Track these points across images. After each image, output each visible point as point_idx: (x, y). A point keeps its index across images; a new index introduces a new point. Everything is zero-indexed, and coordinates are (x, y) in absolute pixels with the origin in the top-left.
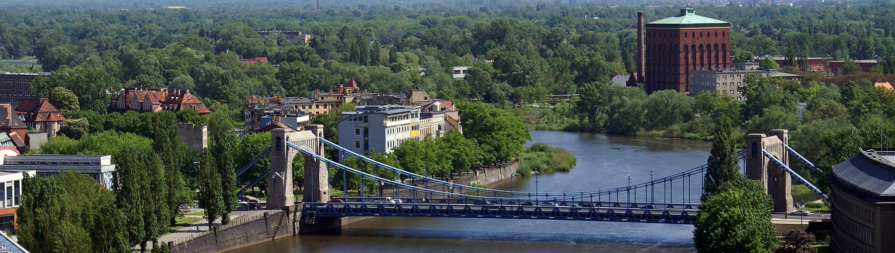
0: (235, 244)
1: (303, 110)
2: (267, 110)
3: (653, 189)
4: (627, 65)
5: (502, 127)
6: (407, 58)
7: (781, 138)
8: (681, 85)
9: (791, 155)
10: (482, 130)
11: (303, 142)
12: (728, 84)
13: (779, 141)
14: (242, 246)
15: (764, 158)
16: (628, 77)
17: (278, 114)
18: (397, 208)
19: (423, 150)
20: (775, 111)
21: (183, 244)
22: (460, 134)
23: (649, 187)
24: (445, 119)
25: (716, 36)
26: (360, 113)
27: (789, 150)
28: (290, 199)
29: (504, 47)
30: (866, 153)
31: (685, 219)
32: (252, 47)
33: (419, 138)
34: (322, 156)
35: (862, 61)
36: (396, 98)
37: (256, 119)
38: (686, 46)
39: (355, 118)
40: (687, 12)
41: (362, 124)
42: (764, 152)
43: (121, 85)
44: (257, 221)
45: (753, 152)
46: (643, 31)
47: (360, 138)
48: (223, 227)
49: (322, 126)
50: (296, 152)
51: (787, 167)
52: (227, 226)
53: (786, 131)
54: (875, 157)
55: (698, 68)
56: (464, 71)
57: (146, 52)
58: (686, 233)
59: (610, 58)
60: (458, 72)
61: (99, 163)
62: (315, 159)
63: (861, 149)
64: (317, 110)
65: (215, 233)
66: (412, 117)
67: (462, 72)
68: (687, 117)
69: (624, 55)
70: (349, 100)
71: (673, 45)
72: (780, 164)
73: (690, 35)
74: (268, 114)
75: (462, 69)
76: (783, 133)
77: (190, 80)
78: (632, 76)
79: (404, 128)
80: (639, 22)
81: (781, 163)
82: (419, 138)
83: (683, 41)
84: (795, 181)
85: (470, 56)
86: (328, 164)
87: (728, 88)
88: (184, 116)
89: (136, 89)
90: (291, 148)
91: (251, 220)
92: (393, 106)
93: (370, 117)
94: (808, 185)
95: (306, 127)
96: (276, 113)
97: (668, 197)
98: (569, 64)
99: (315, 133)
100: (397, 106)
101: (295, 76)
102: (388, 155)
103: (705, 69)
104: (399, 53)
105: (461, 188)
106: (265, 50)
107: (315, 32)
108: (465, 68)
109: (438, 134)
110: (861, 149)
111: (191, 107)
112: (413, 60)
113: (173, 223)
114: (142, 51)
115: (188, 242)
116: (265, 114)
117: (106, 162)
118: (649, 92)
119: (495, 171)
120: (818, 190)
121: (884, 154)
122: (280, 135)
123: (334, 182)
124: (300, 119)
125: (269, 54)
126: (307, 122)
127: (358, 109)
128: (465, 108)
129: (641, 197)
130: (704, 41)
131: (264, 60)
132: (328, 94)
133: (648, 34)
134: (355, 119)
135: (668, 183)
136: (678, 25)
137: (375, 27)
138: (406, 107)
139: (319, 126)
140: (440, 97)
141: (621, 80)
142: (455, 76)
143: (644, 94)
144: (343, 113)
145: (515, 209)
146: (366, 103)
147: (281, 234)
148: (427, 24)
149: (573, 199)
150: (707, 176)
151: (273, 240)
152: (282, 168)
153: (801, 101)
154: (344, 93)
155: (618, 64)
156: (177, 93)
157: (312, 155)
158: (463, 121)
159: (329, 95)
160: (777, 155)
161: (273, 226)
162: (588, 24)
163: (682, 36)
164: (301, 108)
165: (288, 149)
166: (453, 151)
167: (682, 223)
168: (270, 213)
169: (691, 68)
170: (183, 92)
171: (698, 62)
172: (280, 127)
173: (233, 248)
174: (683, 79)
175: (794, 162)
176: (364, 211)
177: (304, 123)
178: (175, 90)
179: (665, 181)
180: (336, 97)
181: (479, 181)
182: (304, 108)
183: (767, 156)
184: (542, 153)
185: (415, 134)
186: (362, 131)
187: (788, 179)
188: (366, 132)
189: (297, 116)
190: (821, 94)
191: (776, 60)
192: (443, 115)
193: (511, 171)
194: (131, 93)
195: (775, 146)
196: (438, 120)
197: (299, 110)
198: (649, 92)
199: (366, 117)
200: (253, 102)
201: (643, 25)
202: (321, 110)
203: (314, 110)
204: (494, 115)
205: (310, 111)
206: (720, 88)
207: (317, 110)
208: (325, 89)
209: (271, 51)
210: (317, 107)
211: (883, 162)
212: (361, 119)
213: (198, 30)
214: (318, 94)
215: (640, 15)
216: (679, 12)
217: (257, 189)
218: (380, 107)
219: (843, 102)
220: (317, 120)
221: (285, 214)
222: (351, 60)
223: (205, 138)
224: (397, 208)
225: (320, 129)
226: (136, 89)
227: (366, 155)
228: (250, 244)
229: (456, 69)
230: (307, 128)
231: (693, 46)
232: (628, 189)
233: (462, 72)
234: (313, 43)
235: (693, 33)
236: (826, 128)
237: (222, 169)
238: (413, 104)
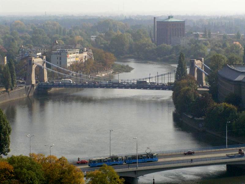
3: (158, 78)
7: (202, 61)
9: (205, 67)
11: (39, 62)
13: (201, 62)
23: (157, 78)
24: (88, 54)
27: (204, 65)
28: (34, 82)
30: (229, 66)
35: (230, 34)
39: (56, 54)
41: (59, 56)
47: (58, 60)
49: (45, 56)
50: (36, 65)
51: (203, 70)
53: (203, 58)
56: (95, 37)
58: (168, 94)
60: (93, 38)
64: (44, 51)
74: (27, 52)
75: (94, 36)
76: (202, 59)
93: (62, 54)
95: (41, 57)
97: (163, 81)
99: (43, 59)
100: (71, 49)
105: (93, 78)
108: (96, 36)
109: (85, 59)
116: (26, 52)
122: (31, 60)
126: (40, 55)
127: (58, 51)
129: (153, 80)
135: (163, 76)
139: (44, 56)
146: (61, 48)
160: (199, 67)
177: (39, 55)
182: (39, 50)
185: (78, 59)
186: (59, 58)
192: (87, 52)
196: (85, 54)
197: (38, 51)
201: (156, 22)
202: (46, 51)
212: (59, 54)
223: (6, 60)
225: (45, 57)
227: (60, 66)
229: (92, 36)
231: (173, 29)
232: (150, 78)
237: (12, 73)
238: (77, 49)
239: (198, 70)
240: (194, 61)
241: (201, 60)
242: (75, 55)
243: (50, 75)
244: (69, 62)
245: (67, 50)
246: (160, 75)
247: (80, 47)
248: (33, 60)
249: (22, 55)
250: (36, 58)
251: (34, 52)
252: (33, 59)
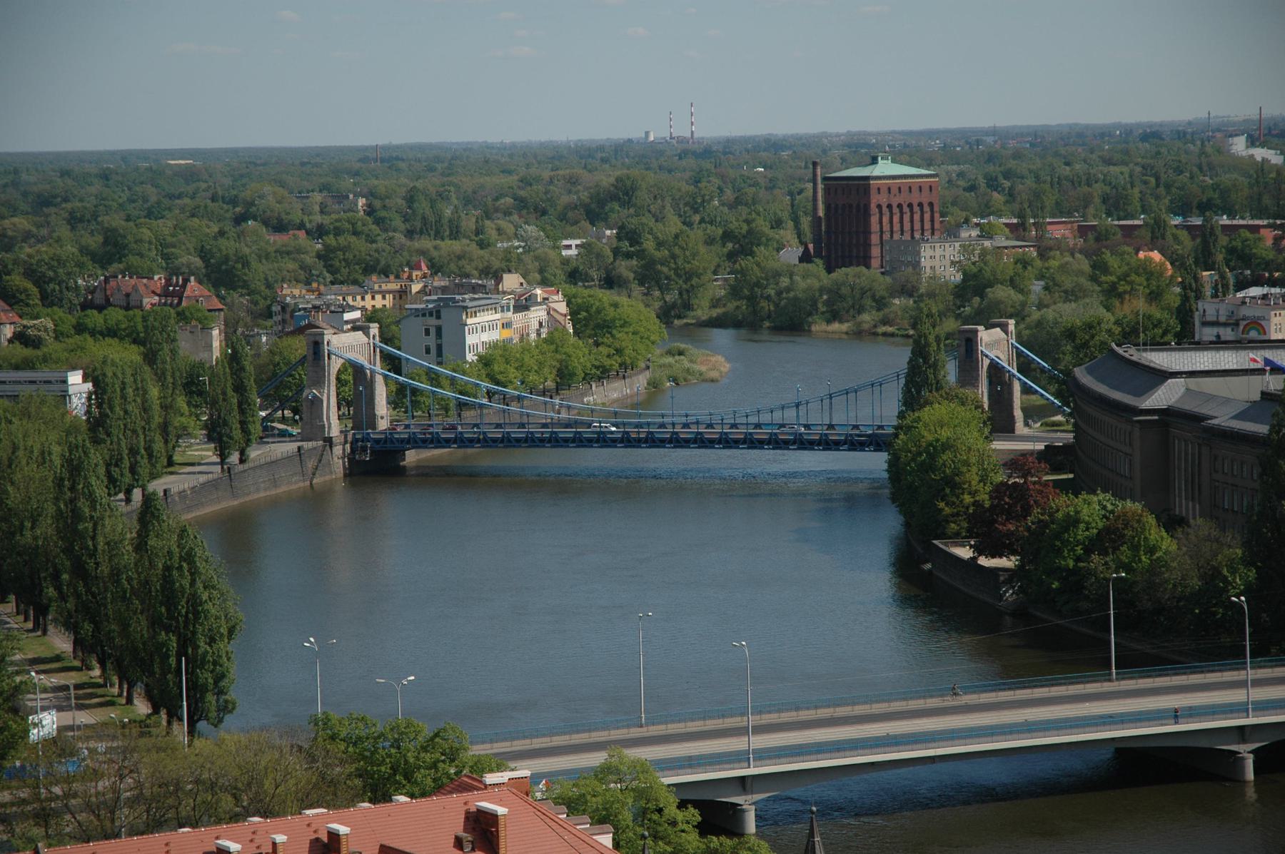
0: (258, 490)
1: (351, 303)
2: (302, 303)
3: (831, 403)
4: (799, 235)
5: (626, 322)
6: (498, 229)
7: (1006, 332)
8: (873, 261)
10: (598, 326)
11: (351, 348)
12: (937, 258)
13: (1003, 335)
14: (268, 493)
15: (982, 360)
16: (801, 249)
17: (317, 308)
18: (481, 437)
19: (518, 355)
20: (1001, 293)
21: (184, 491)
22: (568, 333)
23: (826, 402)
24: (548, 313)
25: (921, 191)
26: (431, 306)
27: (1017, 348)
28: (335, 428)
29: (632, 211)
30: (1120, 351)
31: (876, 442)
32: (284, 216)
33: (511, 339)
34: (378, 368)
35: (1122, 223)
36: (480, 285)
37: (287, 316)
38: (879, 207)
40: (880, 158)
41: (433, 321)
42: (982, 352)
43: (99, 272)
44: (289, 458)
45: (967, 350)
46: (820, 186)
47: (431, 341)
48: (241, 467)
49: (376, 325)
50: (340, 361)
51: (1015, 372)
52: (246, 466)
53: (1012, 322)
54: (1131, 355)
55: (896, 237)
56: (577, 246)
57: (136, 225)
58: (875, 463)
59: (777, 224)
60: (569, 247)
61: (65, 382)
62: (368, 372)
63: (1113, 345)
64: (373, 303)
65: (230, 476)
66: (502, 311)
67: (574, 247)
68: (880, 304)
69: (796, 221)
70: (416, 288)
71: (862, 205)
72: (1004, 367)
73: (884, 190)
74: (305, 309)
77: (197, 262)
78: (806, 249)
79: (492, 327)
80: (815, 175)
81: (1006, 365)
82: (511, 339)
83: (875, 199)
84: (1026, 390)
85: (585, 224)
86: (386, 377)
87: (937, 263)
88: (187, 314)
89: (120, 277)
90: (333, 357)
91: (279, 456)
92: (476, 296)
94: (1042, 395)
96: (315, 307)
97: (852, 414)
98: (720, 231)
99: (367, 335)
101: (344, 254)
102: (470, 363)
103: (907, 237)
104: (488, 223)
105: (569, 407)
106: (302, 221)
107: (371, 194)
108: (578, 242)
109: (539, 335)
110: (1113, 345)
111: (197, 301)
112: (508, 231)
113: (170, 463)
114: (131, 224)
115: (193, 488)
116: (300, 310)
117: (75, 378)
118: (830, 270)
119: (618, 384)
120: (1056, 401)
121: (1145, 350)
122: (317, 338)
123: (394, 403)
124: (347, 316)
125: (308, 225)
126: (357, 320)
127: (428, 301)
128: (575, 296)
129: (817, 417)
130: (903, 199)
131: (301, 234)
132: (387, 280)
133: (827, 190)
134: (424, 315)
135: (852, 395)
136: (867, 178)
137: (455, 185)
138: (493, 296)
139: (371, 325)
140: (544, 283)
141: (791, 254)
142: (564, 253)
143: (823, 273)
144: (407, 306)
145: (642, 436)
146: (439, 291)
147: (321, 476)
148: (526, 182)
149: (722, 420)
150: (906, 385)
151: (311, 484)
152: (319, 381)
153: (1038, 279)
154: (410, 278)
155: (788, 234)
156: (177, 282)
157: (362, 366)
158: (573, 315)
159: (389, 282)
161: (310, 464)
162: (748, 178)
163: (873, 192)
164: (349, 299)
165: (329, 358)
166: (558, 356)
167: (871, 451)
168: (305, 446)
169: (887, 236)
170: (186, 281)
171: (897, 227)
172: (318, 328)
173: (256, 496)
174: (875, 251)
175: (1025, 367)
176: (437, 442)
177: (353, 321)
178: (175, 278)
179: (847, 393)
180: (399, 284)
181: (595, 396)
182: (354, 300)
183: (987, 356)
184: (682, 357)
185: (507, 334)
186: (433, 331)
187: (1017, 387)
188: (439, 330)
189: (343, 312)
190: (1063, 267)
191: (1004, 224)
192: (545, 307)
193: (640, 382)
194: (112, 283)
195: (996, 343)
196: (537, 314)
197: (347, 304)
198: (830, 270)
199: (438, 312)
200: (284, 292)
202: (379, 302)
203: (368, 303)
204: (616, 305)
205: (362, 304)
206: (925, 262)
207: (373, 303)
208: (385, 272)
209: (310, 222)
210: (373, 298)
211: (1143, 362)
212: (431, 315)
213: (209, 194)
214: (375, 281)
215: (815, 164)
216: (869, 160)
217: (287, 413)
218: (458, 297)
219: (1094, 279)
220: (371, 316)
221: (328, 448)
222: (421, 233)
223: (216, 344)
224: (481, 437)
225: (374, 329)
226: (120, 277)
227: (440, 364)
228: (280, 490)
229: (565, 242)
230: (355, 329)
232: (797, 405)
233: (574, 247)
234: (370, 211)
235: (889, 189)
236: (1069, 313)
237: (240, 388)
238: (504, 293)
239: (995, 369)
240: (976, 331)
241: (1004, 328)
242: (498, 316)
243: (400, 397)
244: (475, 346)
245: (466, 296)
246: (840, 393)
247: (517, 286)
248: (326, 338)
249: (284, 321)
250: (339, 330)
251: (333, 308)
252: (329, 336)
